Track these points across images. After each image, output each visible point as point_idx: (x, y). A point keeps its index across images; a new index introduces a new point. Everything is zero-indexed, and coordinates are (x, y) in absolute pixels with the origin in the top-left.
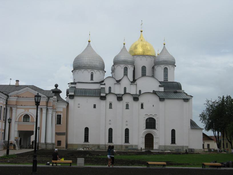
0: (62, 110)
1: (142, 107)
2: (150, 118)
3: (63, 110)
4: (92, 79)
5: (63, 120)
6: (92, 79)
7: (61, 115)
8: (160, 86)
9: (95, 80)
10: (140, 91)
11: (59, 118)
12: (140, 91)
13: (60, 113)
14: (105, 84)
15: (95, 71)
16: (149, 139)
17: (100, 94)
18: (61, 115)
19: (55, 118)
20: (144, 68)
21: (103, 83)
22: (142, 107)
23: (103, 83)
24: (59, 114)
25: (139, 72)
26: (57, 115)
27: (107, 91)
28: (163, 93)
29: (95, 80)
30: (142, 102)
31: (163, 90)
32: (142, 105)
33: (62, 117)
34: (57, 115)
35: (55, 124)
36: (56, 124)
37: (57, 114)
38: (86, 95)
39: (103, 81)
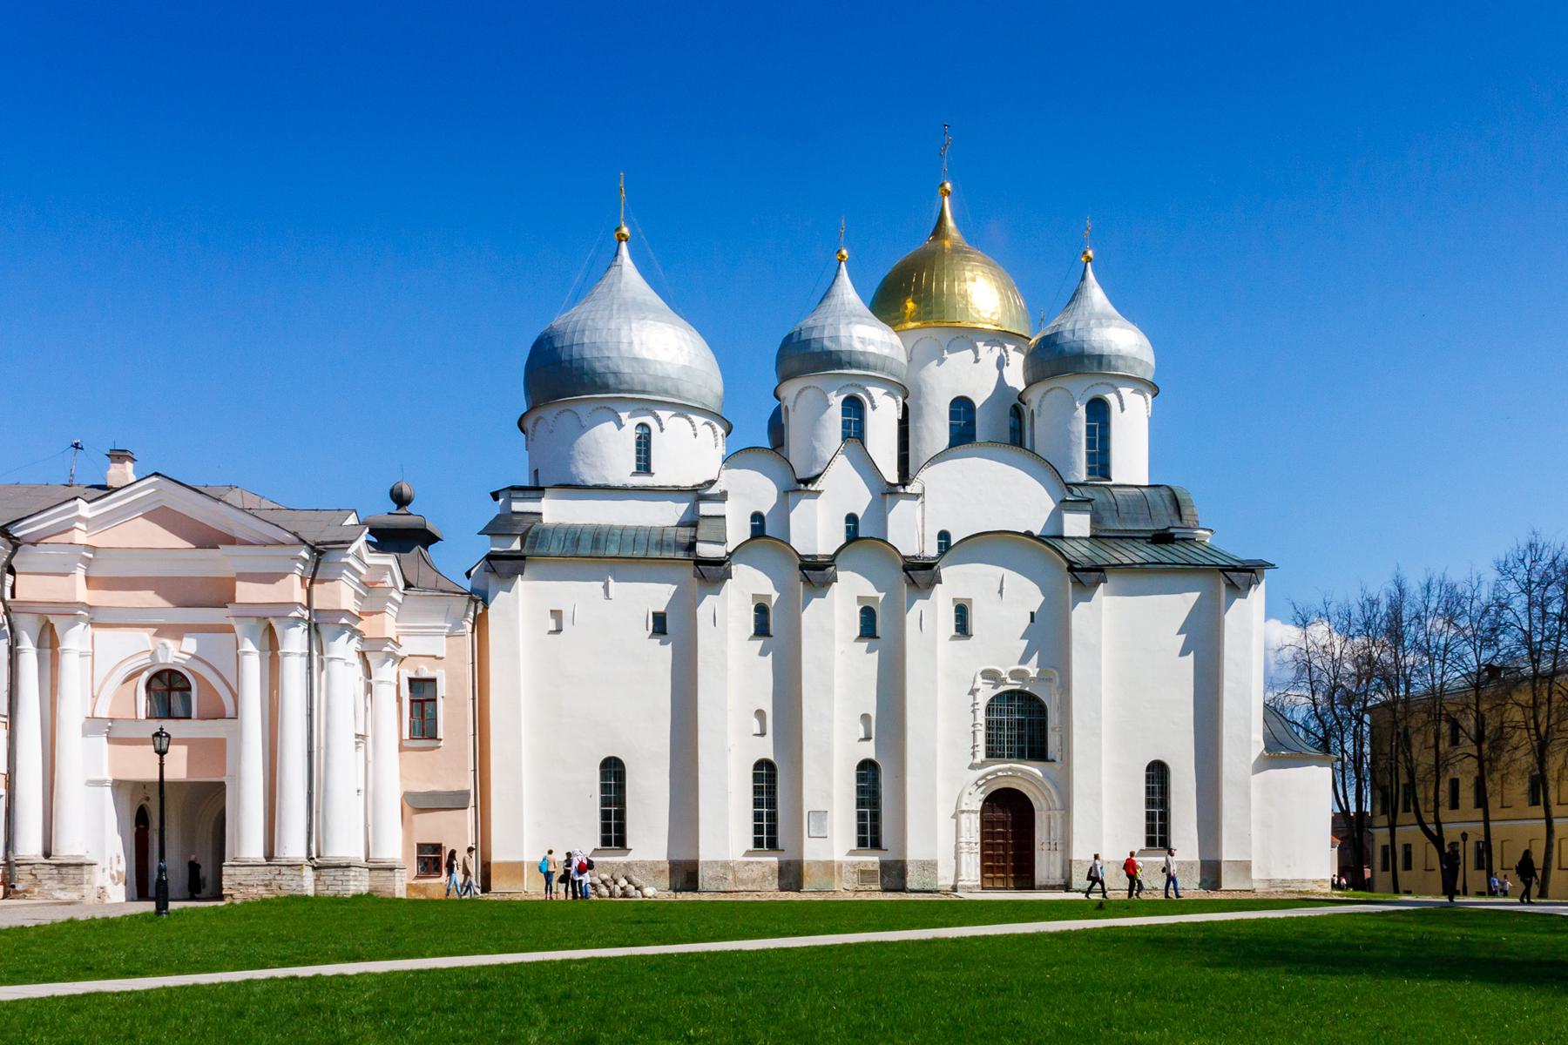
0: (439, 645)
1: (963, 626)
2: (1011, 694)
3: (449, 646)
4: (644, 466)
5: (451, 712)
6: (644, 466)
7: (434, 680)
8: (1064, 505)
9: (663, 474)
10: (944, 536)
11: (422, 693)
12: (944, 536)
13: (432, 668)
14: (722, 497)
15: (664, 415)
16: (1010, 829)
17: (691, 547)
18: (434, 680)
19: (399, 699)
20: (962, 408)
21: (714, 490)
22: (963, 626)
23: (714, 490)
24: (426, 673)
25: (935, 429)
26: (411, 681)
27: (737, 532)
28: (1086, 543)
29: (663, 474)
30: (962, 594)
31: (1086, 532)
32: (962, 614)
33: (442, 689)
34: (411, 681)
35: (401, 740)
36: (406, 735)
37: (407, 673)
38: (600, 553)
39: (712, 483)
